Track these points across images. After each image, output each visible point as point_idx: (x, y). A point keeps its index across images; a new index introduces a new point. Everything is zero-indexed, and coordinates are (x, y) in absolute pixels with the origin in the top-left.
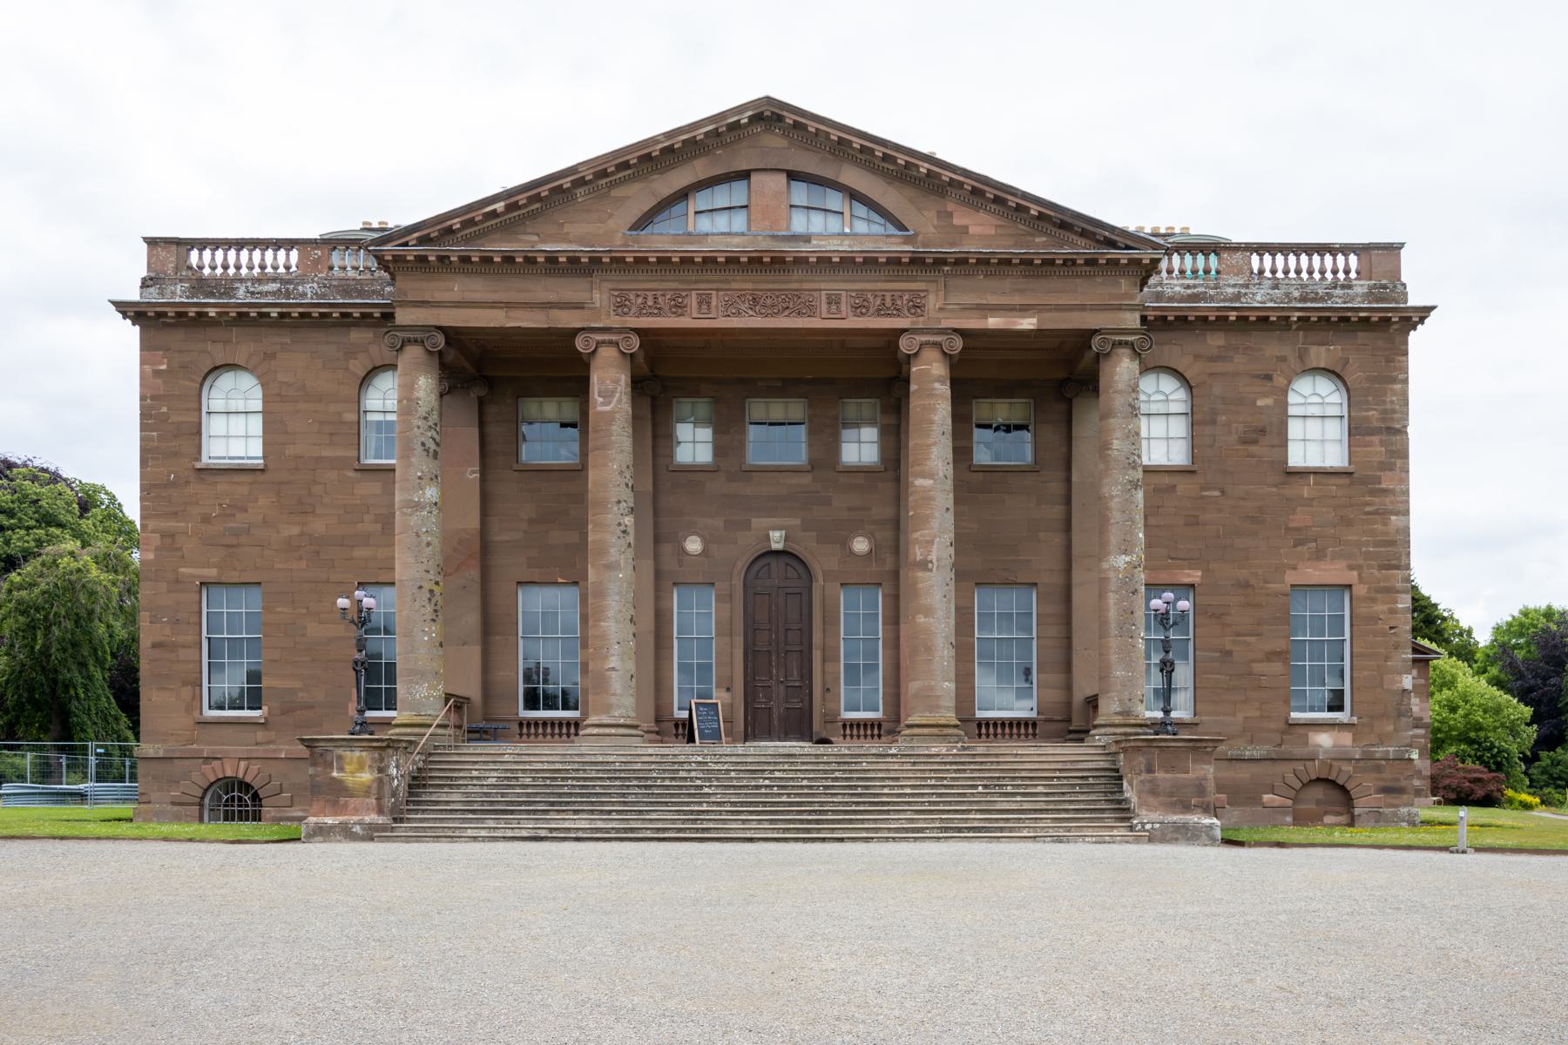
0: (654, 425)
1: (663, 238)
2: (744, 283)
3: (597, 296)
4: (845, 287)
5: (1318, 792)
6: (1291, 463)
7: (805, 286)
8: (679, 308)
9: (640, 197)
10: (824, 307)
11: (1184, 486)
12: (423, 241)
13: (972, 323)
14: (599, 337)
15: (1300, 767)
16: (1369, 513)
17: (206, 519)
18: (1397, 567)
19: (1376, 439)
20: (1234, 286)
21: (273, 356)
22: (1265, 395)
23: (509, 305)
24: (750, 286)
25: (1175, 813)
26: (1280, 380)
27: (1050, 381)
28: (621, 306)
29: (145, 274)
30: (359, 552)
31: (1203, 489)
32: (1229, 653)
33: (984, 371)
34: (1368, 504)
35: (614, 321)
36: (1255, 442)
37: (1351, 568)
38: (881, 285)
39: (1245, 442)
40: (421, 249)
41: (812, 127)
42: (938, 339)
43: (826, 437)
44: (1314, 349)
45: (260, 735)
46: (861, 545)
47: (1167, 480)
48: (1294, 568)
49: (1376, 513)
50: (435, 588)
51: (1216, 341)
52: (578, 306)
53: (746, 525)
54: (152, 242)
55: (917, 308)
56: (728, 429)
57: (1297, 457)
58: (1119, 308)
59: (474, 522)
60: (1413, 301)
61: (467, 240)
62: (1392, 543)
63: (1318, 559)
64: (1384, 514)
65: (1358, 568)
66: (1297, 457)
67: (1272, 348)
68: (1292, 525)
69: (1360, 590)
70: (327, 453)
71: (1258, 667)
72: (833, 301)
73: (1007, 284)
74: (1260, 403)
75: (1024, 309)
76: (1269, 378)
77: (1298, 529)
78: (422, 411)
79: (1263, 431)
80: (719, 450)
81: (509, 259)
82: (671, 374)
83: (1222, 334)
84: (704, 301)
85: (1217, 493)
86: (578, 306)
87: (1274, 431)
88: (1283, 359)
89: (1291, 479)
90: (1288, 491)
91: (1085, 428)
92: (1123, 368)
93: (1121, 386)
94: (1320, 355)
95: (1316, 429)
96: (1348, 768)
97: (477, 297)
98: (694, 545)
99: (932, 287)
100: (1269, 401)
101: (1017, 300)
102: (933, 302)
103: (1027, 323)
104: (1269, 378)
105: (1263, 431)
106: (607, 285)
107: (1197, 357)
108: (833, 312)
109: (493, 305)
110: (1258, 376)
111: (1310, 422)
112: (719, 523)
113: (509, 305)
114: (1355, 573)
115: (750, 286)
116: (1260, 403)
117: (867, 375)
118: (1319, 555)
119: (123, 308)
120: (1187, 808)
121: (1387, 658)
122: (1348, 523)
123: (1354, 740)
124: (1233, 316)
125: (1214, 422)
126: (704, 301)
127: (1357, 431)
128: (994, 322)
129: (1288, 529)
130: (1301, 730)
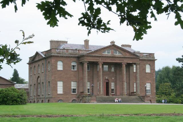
8: (106, 60)
17: (58, 75)
27: (129, 65)
28: (102, 60)
30: (72, 78)
35: (102, 61)
41: (117, 46)
45: (63, 95)
52: (98, 60)
60: (155, 59)
67: (145, 62)
69: (152, 83)
70: (69, 69)
75: (131, 61)
86: (98, 60)
87: (145, 69)
103: (131, 62)
113: (93, 59)
127: (151, 69)
128: (129, 62)
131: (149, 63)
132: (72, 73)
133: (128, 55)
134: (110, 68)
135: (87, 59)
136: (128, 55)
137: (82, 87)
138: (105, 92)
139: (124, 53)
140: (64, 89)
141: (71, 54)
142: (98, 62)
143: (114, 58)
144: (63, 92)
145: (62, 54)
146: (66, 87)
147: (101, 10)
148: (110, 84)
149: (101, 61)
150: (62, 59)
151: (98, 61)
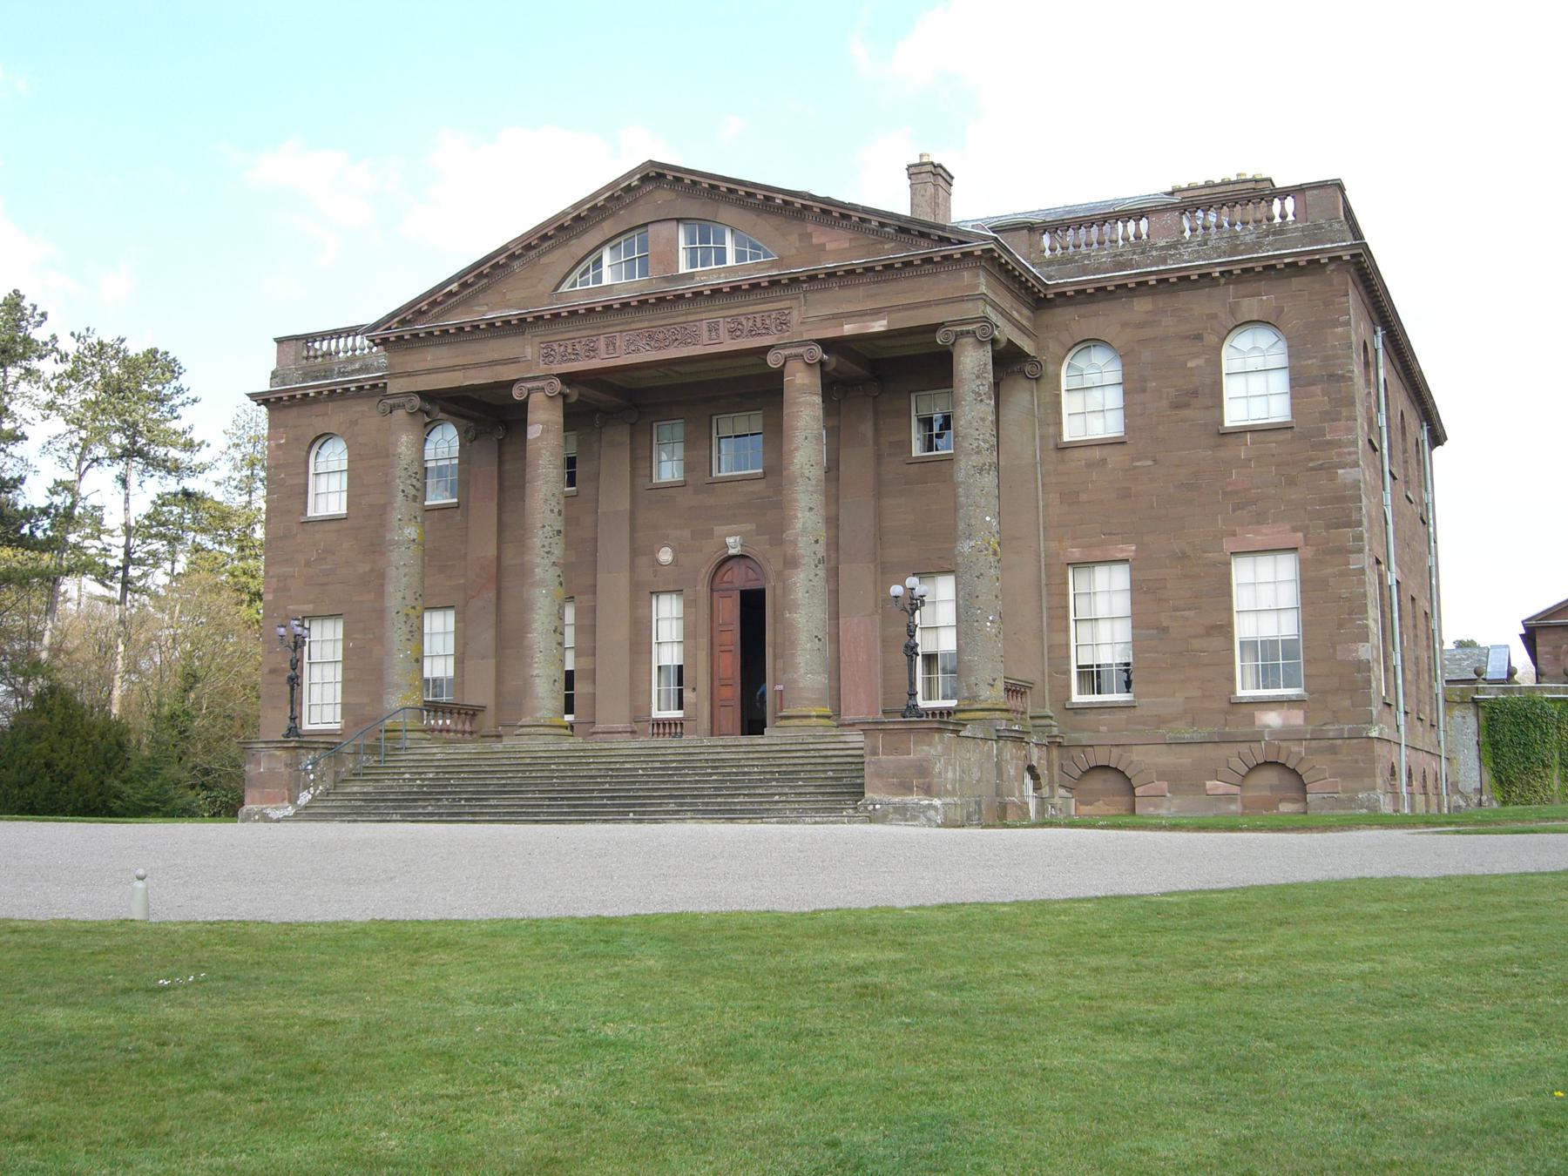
0: (632, 450)
1: (576, 291)
2: (642, 322)
3: (529, 350)
4: (720, 314)
5: (1270, 777)
6: (1227, 424)
7: (690, 318)
9: (559, 259)
10: (705, 335)
11: (1115, 457)
12: (403, 322)
14: (529, 385)
15: (1244, 748)
16: (1312, 469)
18: (1348, 525)
19: (1318, 389)
20: (1162, 248)
21: (356, 423)
22: (1195, 356)
23: (464, 367)
24: (646, 324)
25: (896, 795)
26: (1212, 339)
29: (274, 367)
31: (1133, 460)
32: (1165, 630)
34: (1312, 460)
35: (542, 369)
36: (1187, 405)
37: (1295, 530)
38: (751, 309)
39: (1177, 406)
40: (398, 331)
42: (800, 350)
44: (1245, 302)
47: (1097, 453)
48: (1234, 535)
49: (1320, 468)
50: (411, 612)
51: (1142, 306)
52: (515, 361)
53: (709, 533)
54: (279, 341)
55: (783, 324)
57: (1235, 414)
58: (962, 299)
59: (493, 552)
61: (436, 318)
62: (1341, 499)
63: (1258, 523)
64: (1330, 469)
65: (1304, 529)
66: (1235, 414)
67: (1200, 305)
68: (1229, 489)
71: (1197, 644)
72: (713, 328)
73: (861, 291)
74: (1189, 365)
75: (875, 313)
76: (1199, 337)
77: (1235, 493)
78: (404, 463)
79: (1195, 393)
80: (689, 468)
81: (460, 329)
83: (1149, 299)
84: (611, 344)
85: (1150, 463)
86: (515, 361)
88: (1214, 316)
89: (1226, 439)
90: (1224, 454)
93: (965, 375)
94: (1251, 306)
96: (1295, 748)
97: (441, 363)
98: (665, 556)
99: (794, 303)
100: (1200, 362)
101: (869, 305)
102: (795, 317)
103: (879, 326)
104: (1199, 337)
105: (1195, 393)
106: (538, 339)
107: (1125, 325)
108: (712, 337)
109: (452, 369)
110: (1187, 337)
111: (1252, 378)
112: (687, 533)
113: (464, 367)
114: (1300, 535)
115: (646, 324)
116: (1189, 365)
118: (1260, 519)
119: (260, 398)
120: (907, 788)
121: (1340, 626)
122: (1292, 482)
123: (1306, 719)
124: (1152, 280)
125: (1144, 390)
126: (611, 344)
127: (1299, 383)
128: (849, 329)
129: (1225, 493)
130: (1244, 709)
135: (409, 374)
136: (837, 250)
137: (491, 663)
140: (346, 682)
142: (511, 383)
143: (679, 315)
145: (343, 374)
149: (532, 366)
151: (506, 373)
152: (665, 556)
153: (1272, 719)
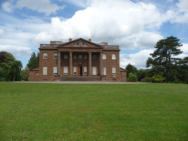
9: (73, 44)
13: (92, 51)
33: (93, 54)
39: (109, 58)
43: (83, 57)
46: (86, 64)
56: (77, 57)
57: (113, 59)
66: (113, 59)
82: (74, 53)
91: (99, 57)
92: (101, 54)
95: (114, 57)
103: (96, 51)
117: (87, 54)
118: (114, 65)
128: (94, 51)
131: (114, 52)
132: (54, 60)
133: (93, 46)
134: (83, 57)
136: (93, 46)
138: (80, 74)
139: (90, 45)
140: (47, 71)
141: (43, 47)
144: (47, 73)
146: (50, 71)
147: (71, 17)
148: (83, 69)
150: (46, 51)
152: (75, 64)
153: (114, 76)
